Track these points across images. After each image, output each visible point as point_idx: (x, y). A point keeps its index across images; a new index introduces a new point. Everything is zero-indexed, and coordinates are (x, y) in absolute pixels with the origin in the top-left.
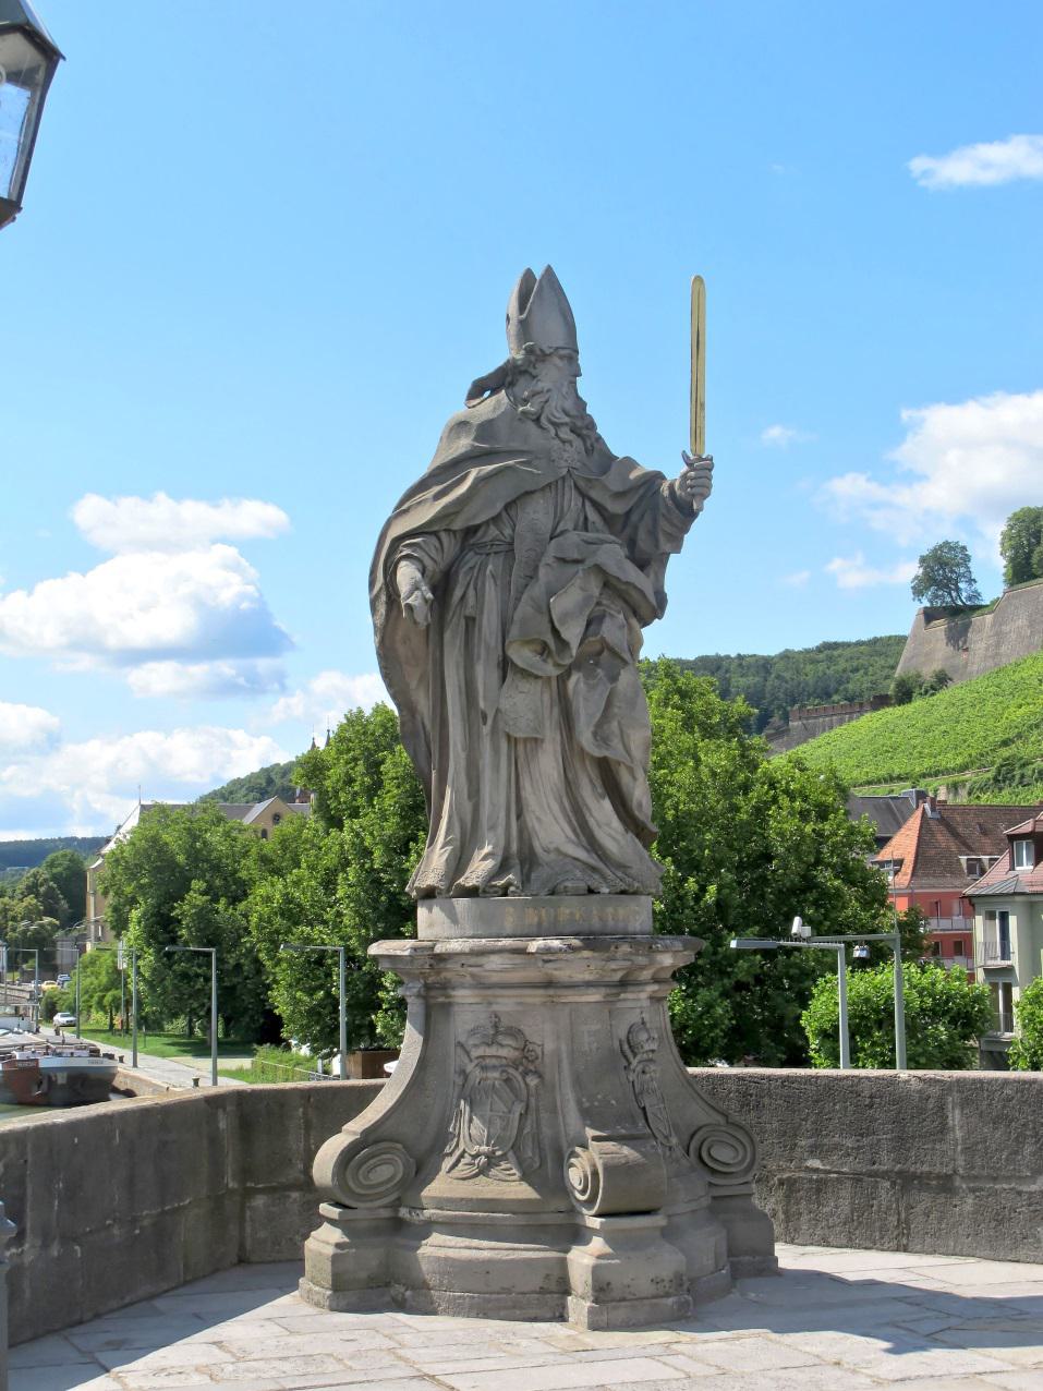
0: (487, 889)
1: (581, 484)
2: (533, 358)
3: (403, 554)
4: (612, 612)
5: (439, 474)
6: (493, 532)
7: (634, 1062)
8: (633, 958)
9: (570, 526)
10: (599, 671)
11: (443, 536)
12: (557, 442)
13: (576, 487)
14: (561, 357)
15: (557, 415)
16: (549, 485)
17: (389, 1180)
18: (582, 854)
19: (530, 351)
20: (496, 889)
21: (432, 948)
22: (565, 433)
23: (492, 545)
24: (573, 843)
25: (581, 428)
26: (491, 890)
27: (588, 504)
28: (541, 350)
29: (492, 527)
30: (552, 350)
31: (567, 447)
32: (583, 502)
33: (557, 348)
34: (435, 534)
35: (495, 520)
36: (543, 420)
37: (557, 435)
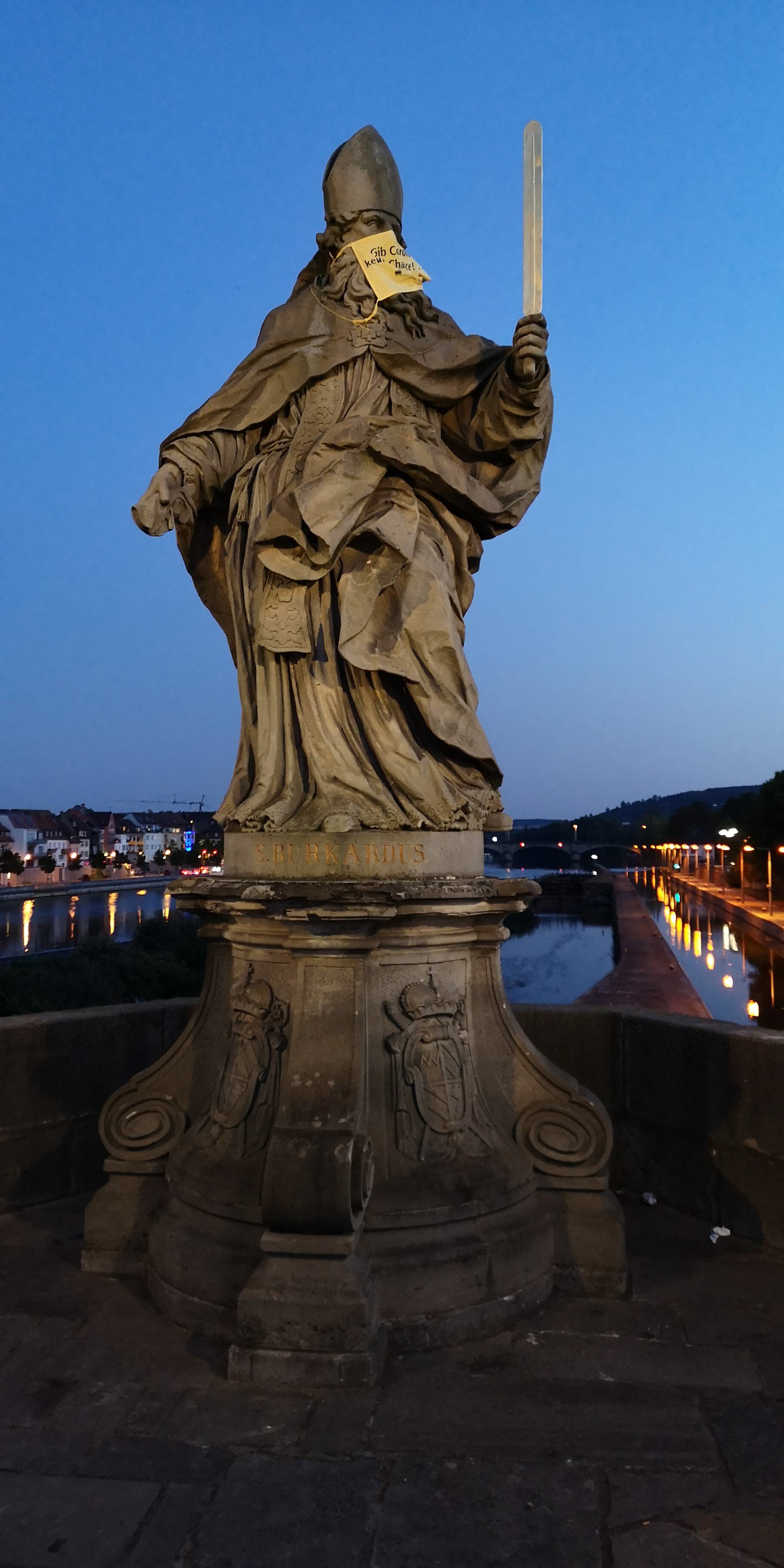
0: (248, 823)
1: (383, 363)
4: (403, 504)
7: (410, 1028)
8: (370, 909)
11: (218, 437)
13: (379, 368)
14: (367, 222)
17: (159, 1129)
18: (362, 783)
19: (331, 221)
23: (280, 444)
24: (354, 771)
27: (394, 387)
28: (343, 217)
29: (279, 422)
30: (354, 215)
32: (389, 385)
33: (361, 212)
36: (346, 297)
37: (359, 312)
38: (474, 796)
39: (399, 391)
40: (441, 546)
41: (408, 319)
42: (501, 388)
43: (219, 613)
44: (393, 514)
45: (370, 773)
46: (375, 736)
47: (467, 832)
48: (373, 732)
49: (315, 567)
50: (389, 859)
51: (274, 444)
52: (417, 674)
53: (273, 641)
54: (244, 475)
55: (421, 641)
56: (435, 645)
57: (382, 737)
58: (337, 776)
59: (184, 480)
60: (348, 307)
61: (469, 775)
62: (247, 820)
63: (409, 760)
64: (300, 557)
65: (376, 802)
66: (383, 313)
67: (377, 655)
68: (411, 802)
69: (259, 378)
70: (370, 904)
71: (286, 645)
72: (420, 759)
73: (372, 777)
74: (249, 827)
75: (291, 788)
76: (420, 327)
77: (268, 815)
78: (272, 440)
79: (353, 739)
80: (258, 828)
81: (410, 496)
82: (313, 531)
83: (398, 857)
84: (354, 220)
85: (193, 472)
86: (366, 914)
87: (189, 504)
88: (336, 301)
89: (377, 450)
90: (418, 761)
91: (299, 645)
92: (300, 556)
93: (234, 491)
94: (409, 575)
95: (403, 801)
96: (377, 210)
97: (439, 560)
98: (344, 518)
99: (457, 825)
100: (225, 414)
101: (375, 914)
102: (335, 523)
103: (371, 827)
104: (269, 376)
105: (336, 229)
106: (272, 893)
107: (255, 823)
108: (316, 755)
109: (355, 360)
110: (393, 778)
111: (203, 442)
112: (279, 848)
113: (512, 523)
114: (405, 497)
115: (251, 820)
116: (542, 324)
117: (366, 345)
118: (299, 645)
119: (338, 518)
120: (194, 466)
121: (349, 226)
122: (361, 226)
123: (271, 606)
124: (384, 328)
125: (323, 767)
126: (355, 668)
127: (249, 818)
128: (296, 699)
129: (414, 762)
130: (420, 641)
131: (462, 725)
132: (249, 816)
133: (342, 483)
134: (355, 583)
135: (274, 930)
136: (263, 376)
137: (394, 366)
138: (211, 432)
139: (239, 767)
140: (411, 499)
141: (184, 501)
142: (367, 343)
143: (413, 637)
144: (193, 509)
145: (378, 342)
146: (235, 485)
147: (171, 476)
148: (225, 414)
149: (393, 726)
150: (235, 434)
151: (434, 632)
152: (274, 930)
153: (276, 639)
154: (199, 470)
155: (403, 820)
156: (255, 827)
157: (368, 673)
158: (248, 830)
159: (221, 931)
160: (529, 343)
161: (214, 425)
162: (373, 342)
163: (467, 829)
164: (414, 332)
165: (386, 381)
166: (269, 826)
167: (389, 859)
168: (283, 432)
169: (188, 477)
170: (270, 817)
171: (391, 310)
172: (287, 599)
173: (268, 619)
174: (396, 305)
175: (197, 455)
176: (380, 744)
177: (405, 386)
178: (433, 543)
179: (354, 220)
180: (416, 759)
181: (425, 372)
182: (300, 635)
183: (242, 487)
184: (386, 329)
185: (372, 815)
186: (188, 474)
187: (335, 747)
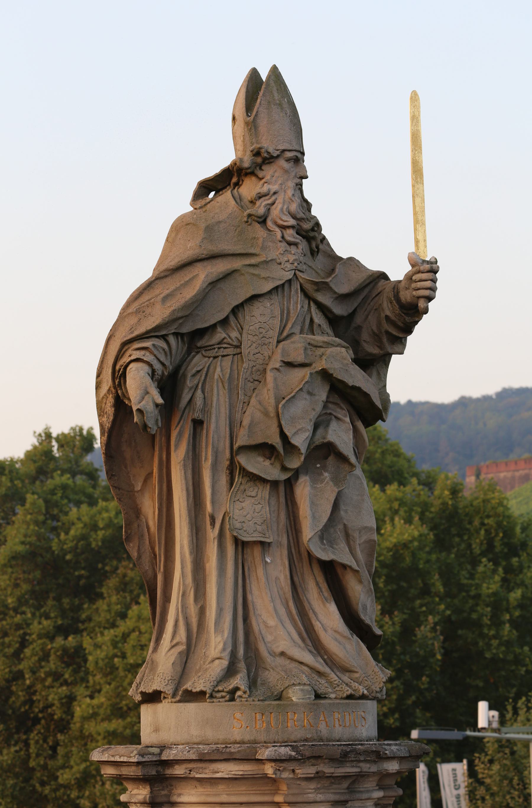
0: (214, 694)
2: (259, 160)
3: (133, 358)
4: (340, 416)
5: (166, 276)
6: (220, 334)
8: (361, 764)
9: (297, 329)
10: (326, 474)
11: (172, 340)
12: (284, 244)
13: (302, 289)
14: (288, 160)
15: (285, 218)
16: (276, 288)
18: (308, 658)
20: (224, 694)
21: (160, 754)
23: (219, 348)
24: (300, 647)
25: (307, 231)
26: (219, 695)
27: (313, 307)
28: (268, 153)
29: (219, 329)
30: (278, 153)
31: (293, 249)
33: (284, 151)
34: (164, 337)
35: (224, 322)
36: (269, 223)
37: (283, 237)
39: (317, 311)
42: (388, 313)
43: (119, 489)
49: (284, 469)
50: (348, 724)
51: (213, 347)
53: (242, 531)
54: (194, 375)
55: (356, 535)
56: (364, 538)
58: (285, 651)
60: (269, 230)
62: (213, 690)
63: (345, 637)
64: (270, 460)
65: (320, 674)
66: (301, 240)
69: (207, 291)
70: (365, 761)
71: (253, 535)
74: (216, 697)
77: (239, 686)
78: (211, 343)
81: (343, 409)
83: (352, 722)
84: (278, 156)
85: (160, 373)
86: (357, 770)
88: (259, 223)
89: (331, 373)
93: (186, 391)
101: (365, 770)
103: (322, 696)
104: (214, 287)
106: (293, 754)
107: (224, 694)
112: (258, 716)
114: (339, 410)
115: (219, 691)
116: (435, 271)
121: (271, 160)
122: (282, 162)
125: (269, 642)
127: (216, 689)
128: (248, 581)
129: (349, 639)
130: (355, 535)
132: (215, 687)
133: (306, 399)
135: (254, 789)
137: (317, 290)
138: (166, 335)
139: (175, 642)
140: (344, 411)
142: (294, 268)
143: (350, 532)
148: (181, 321)
151: (366, 527)
152: (254, 789)
154: (164, 370)
156: (223, 697)
158: (215, 700)
159: (168, 796)
162: (299, 267)
165: (307, 302)
167: (348, 724)
170: (243, 687)
172: (253, 494)
176: (320, 622)
177: (321, 307)
179: (278, 156)
183: (195, 387)
185: (321, 685)
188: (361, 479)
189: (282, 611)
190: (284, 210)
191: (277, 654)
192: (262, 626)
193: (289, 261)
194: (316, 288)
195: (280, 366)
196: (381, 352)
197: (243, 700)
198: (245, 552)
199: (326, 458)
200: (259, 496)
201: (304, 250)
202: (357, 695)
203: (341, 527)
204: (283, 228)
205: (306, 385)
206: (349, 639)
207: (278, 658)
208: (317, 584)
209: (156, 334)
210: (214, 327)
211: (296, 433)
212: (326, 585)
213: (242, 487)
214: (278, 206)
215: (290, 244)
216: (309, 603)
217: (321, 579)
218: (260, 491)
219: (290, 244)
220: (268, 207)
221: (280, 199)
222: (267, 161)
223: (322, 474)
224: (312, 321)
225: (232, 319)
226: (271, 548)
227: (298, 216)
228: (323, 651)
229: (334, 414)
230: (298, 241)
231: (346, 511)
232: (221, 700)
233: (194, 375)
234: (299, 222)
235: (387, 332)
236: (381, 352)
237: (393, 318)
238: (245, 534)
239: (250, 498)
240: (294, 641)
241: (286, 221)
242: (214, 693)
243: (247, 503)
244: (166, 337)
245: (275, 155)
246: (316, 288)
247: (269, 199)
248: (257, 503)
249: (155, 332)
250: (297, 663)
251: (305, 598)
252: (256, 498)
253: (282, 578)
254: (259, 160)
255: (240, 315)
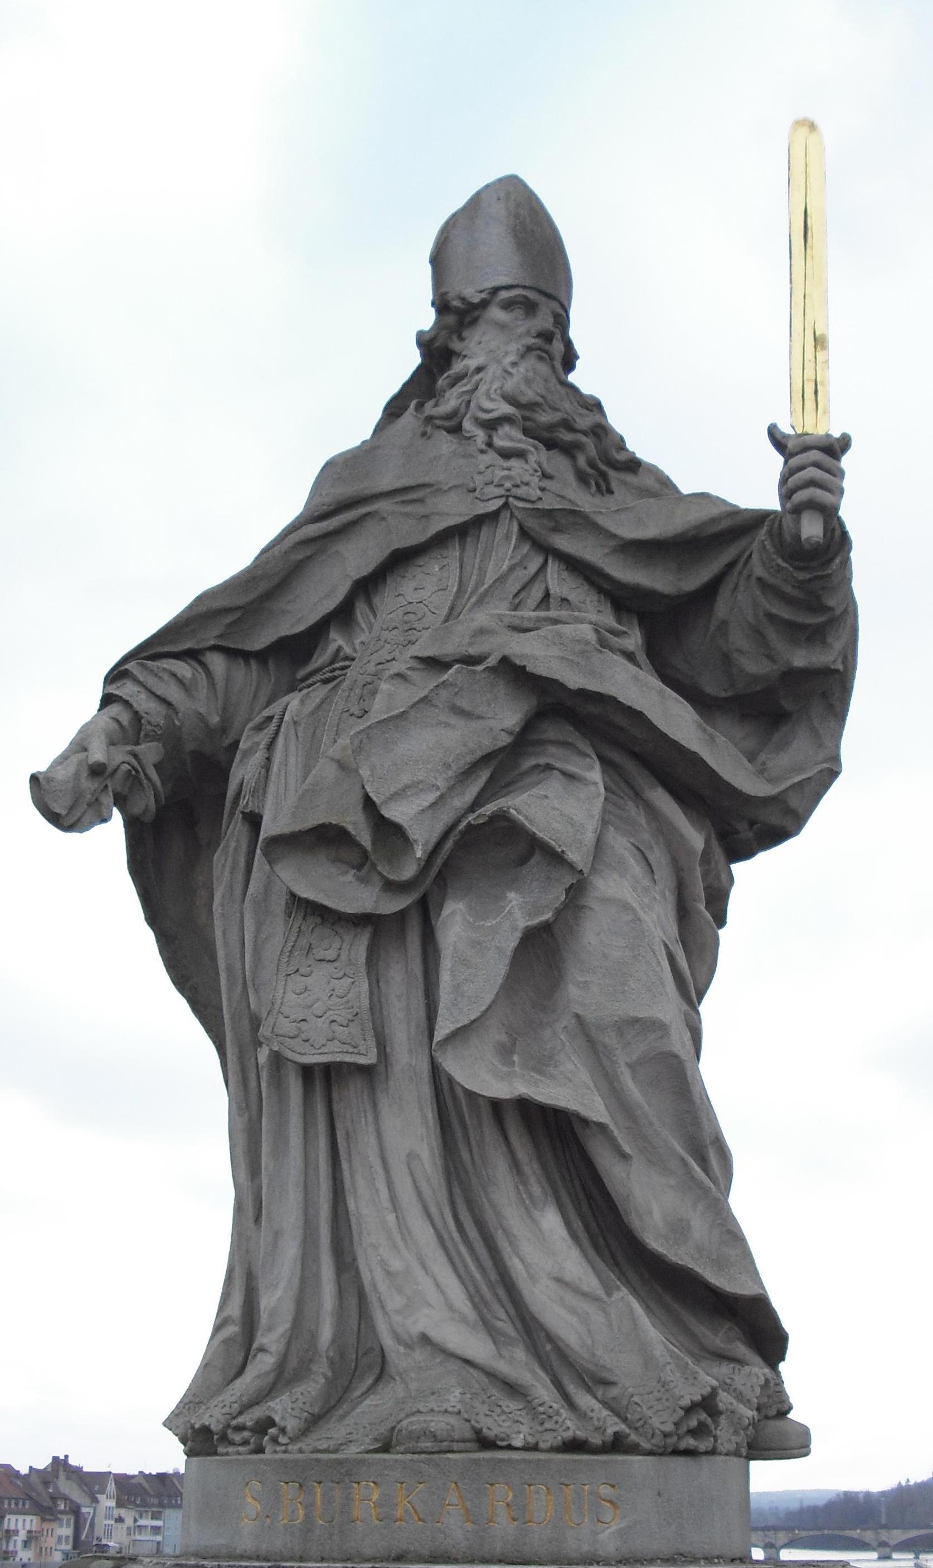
0: (231, 1435)
1: (531, 523)
4: (571, 768)
11: (217, 662)
12: (492, 457)
13: (524, 533)
14: (508, 305)
19: (442, 305)
22: (508, 437)
24: (464, 1320)
25: (551, 427)
26: (237, 1438)
27: (553, 568)
28: (463, 299)
30: (483, 295)
31: (514, 463)
33: (496, 290)
36: (467, 425)
37: (490, 444)
38: (728, 1381)
39: (565, 574)
40: (647, 853)
41: (582, 461)
42: (759, 571)
44: (553, 787)
45: (499, 1324)
46: (511, 1243)
47: (712, 1458)
48: (507, 1233)
49: (391, 887)
52: (602, 1108)
53: (298, 1040)
55: (610, 1039)
56: (640, 1048)
57: (527, 1248)
59: (142, 734)
61: (716, 1335)
62: (228, 1426)
65: (512, 1389)
66: (536, 448)
67: (517, 1069)
68: (589, 1390)
69: (300, 556)
71: (324, 1050)
72: (609, 1294)
73: (504, 1334)
74: (231, 1443)
75: (328, 1358)
76: (604, 475)
77: (273, 1415)
79: (463, 1249)
80: (252, 1446)
81: (586, 755)
82: (386, 812)
84: (484, 304)
87: (149, 779)
90: (606, 1298)
91: (351, 1050)
92: (359, 867)
94: (583, 907)
95: (571, 1388)
96: (525, 287)
97: (646, 882)
98: (451, 788)
99: (690, 1442)
100: (230, 619)
102: (431, 797)
103: (499, 1443)
105: (451, 319)
107: (246, 1434)
108: (383, 1287)
109: (479, 521)
110: (550, 1338)
111: (184, 669)
113: (788, 823)
114: (577, 758)
117: (501, 497)
118: (351, 1050)
119: (438, 788)
120: (162, 709)
122: (496, 313)
123: (298, 970)
124: (536, 471)
125: (398, 1312)
126: (471, 1095)
127: (234, 1423)
128: (345, 1166)
129: (597, 1299)
130: (607, 1040)
131: (699, 1226)
132: (234, 1418)
133: (447, 725)
134: (471, 920)
136: (307, 552)
137: (556, 529)
140: (588, 760)
141: (137, 771)
142: (503, 492)
144: (155, 789)
145: (521, 492)
146: (242, 746)
147: (116, 726)
148: (230, 619)
149: (551, 1220)
150: (245, 656)
151: (637, 1020)
153: (304, 1036)
154: (174, 716)
155: (571, 1428)
156: (245, 1442)
157: (496, 1106)
160: (812, 483)
161: (210, 637)
163: (712, 1452)
164: (593, 482)
166: (275, 1440)
168: (339, 649)
169: (149, 727)
170: (277, 1419)
171: (550, 445)
172: (331, 954)
173: (291, 997)
174: (561, 436)
175: (173, 693)
176: (522, 1260)
177: (574, 565)
178: (633, 848)
179: (484, 304)
180: (600, 1292)
181: (612, 543)
182: (355, 1029)
184: (539, 473)
186: (149, 723)
187: (424, 1267)
188: (633, 910)
189: (424, 1234)
190: (492, 391)
191: (415, 1339)
192: (379, 1275)
193: (492, 482)
194: (551, 524)
195: (409, 669)
196: (775, 667)
197: (278, 1449)
198: (335, 1096)
199: (523, 860)
200: (344, 957)
201: (545, 466)
202: (596, 1440)
203: (566, 1021)
204: (491, 425)
205: (444, 694)
206: (597, 1299)
207: (418, 1352)
208: (515, 1165)
209: (166, 649)
210: (318, 632)
211: (397, 796)
212: (536, 1166)
213: (303, 942)
214: (483, 388)
215: (506, 454)
216: (498, 1214)
217: (524, 1152)
218: (346, 946)
219: (506, 454)
220: (466, 397)
221: (487, 375)
222: (468, 319)
223: (505, 898)
224: (547, 595)
225: (361, 609)
226: (391, 1083)
227: (523, 400)
228: (543, 1334)
229: (558, 765)
230: (522, 446)
231: (585, 986)
232: (241, 1449)
233: (259, 728)
234: (528, 414)
235: (771, 617)
236: (775, 667)
237: (772, 580)
238: (306, 1048)
239: (324, 964)
240: (451, 1307)
241: (492, 410)
242: (229, 1431)
243: (319, 979)
244: (203, 659)
245: (476, 300)
246: (551, 524)
247: (468, 383)
248: (339, 975)
249: (163, 644)
250: (458, 1362)
251: (484, 1200)
252: (337, 964)
253: (425, 1154)
254: (451, 319)
255: (376, 601)
